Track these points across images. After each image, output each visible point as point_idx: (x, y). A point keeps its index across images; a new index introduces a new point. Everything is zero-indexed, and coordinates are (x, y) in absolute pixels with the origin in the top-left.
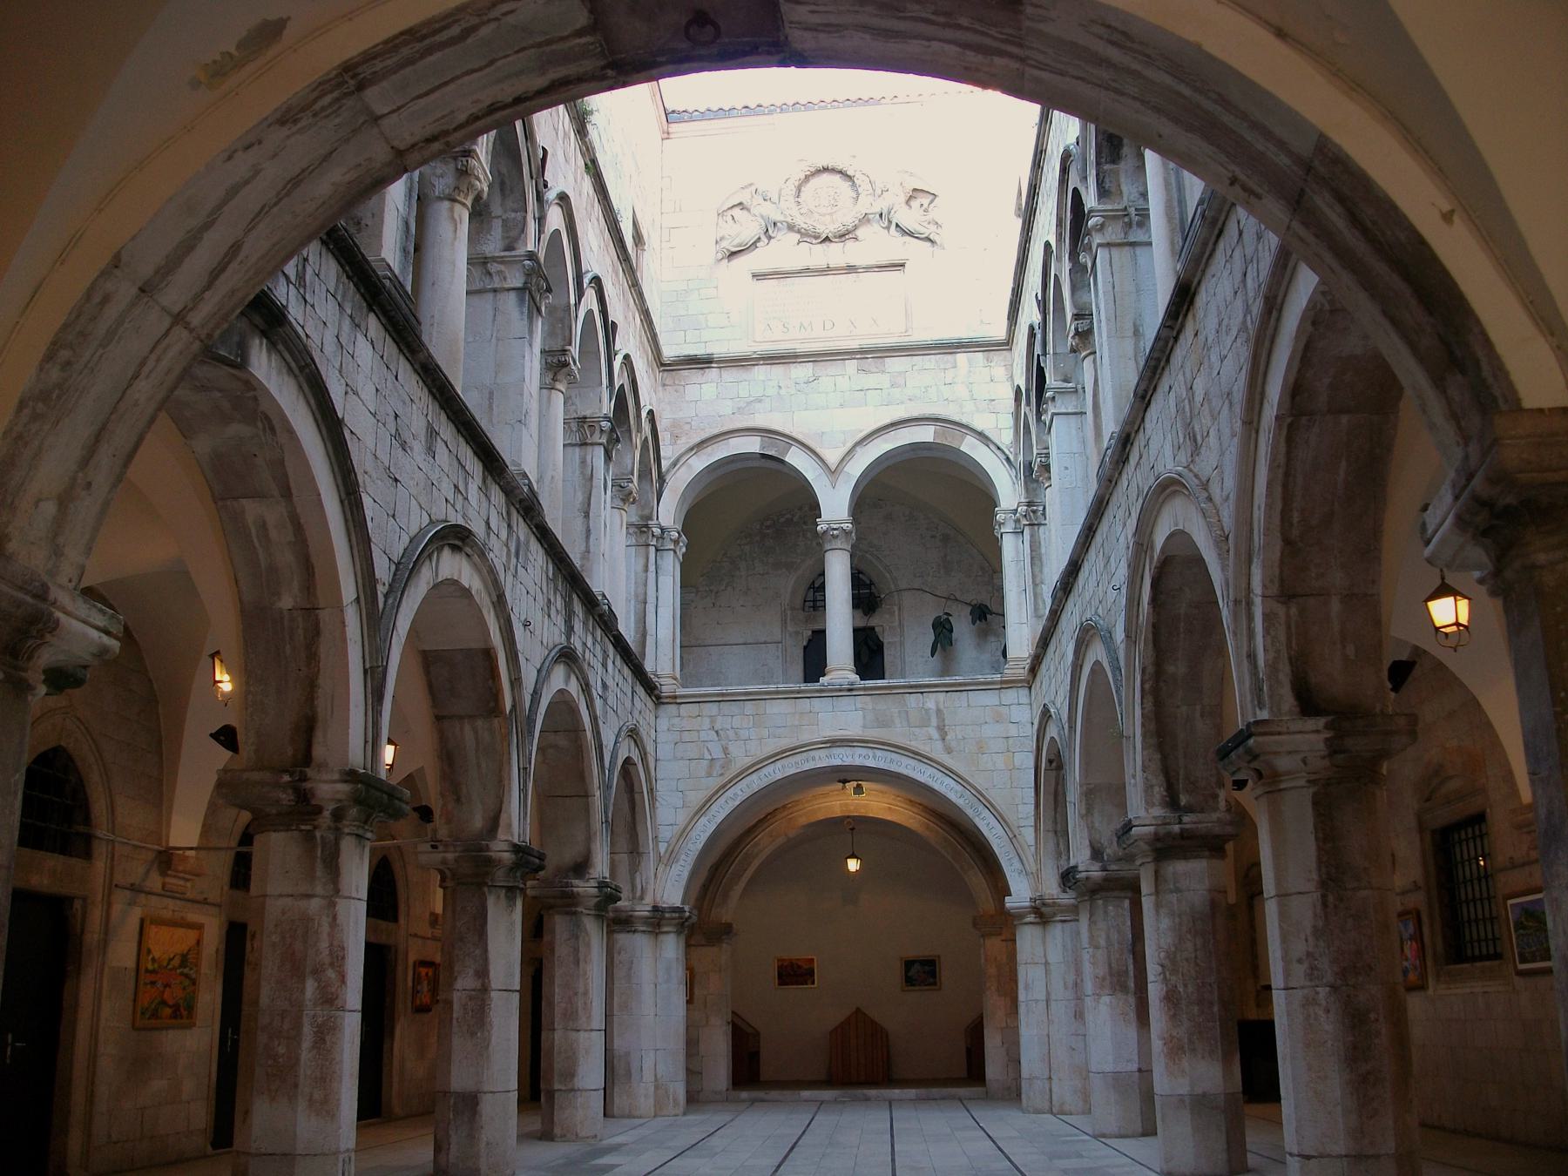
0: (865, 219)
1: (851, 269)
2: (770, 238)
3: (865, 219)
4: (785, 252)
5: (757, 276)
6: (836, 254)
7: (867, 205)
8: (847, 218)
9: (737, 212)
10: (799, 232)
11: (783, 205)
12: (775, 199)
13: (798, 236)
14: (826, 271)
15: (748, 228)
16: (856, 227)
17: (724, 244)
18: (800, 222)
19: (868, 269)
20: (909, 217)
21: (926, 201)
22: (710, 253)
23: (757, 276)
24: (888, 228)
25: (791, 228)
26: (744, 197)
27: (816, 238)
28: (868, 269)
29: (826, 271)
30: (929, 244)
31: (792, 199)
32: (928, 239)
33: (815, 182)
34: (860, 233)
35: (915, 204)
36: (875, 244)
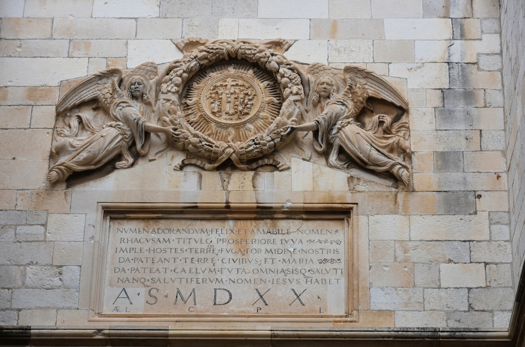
0: (289, 140)
1: (264, 213)
2: (137, 156)
3: (289, 140)
4: (163, 179)
5: (114, 213)
6: (240, 189)
7: (290, 113)
8: (260, 134)
9: (87, 114)
10: (184, 150)
11: (161, 105)
12: (151, 96)
13: (179, 159)
14: (223, 213)
15: (105, 135)
16: (275, 150)
17: (63, 159)
18: (189, 133)
19: (293, 214)
20: (357, 136)
21: (388, 119)
22: (36, 171)
23: (114, 213)
24: (325, 154)
25: (173, 143)
26: (103, 90)
27: (211, 161)
28: (293, 214)
29: (223, 213)
30: (389, 183)
31: (174, 98)
32: (389, 175)
33: (214, 77)
34: (283, 159)
35: (371, 120)
36: (304, 178)
